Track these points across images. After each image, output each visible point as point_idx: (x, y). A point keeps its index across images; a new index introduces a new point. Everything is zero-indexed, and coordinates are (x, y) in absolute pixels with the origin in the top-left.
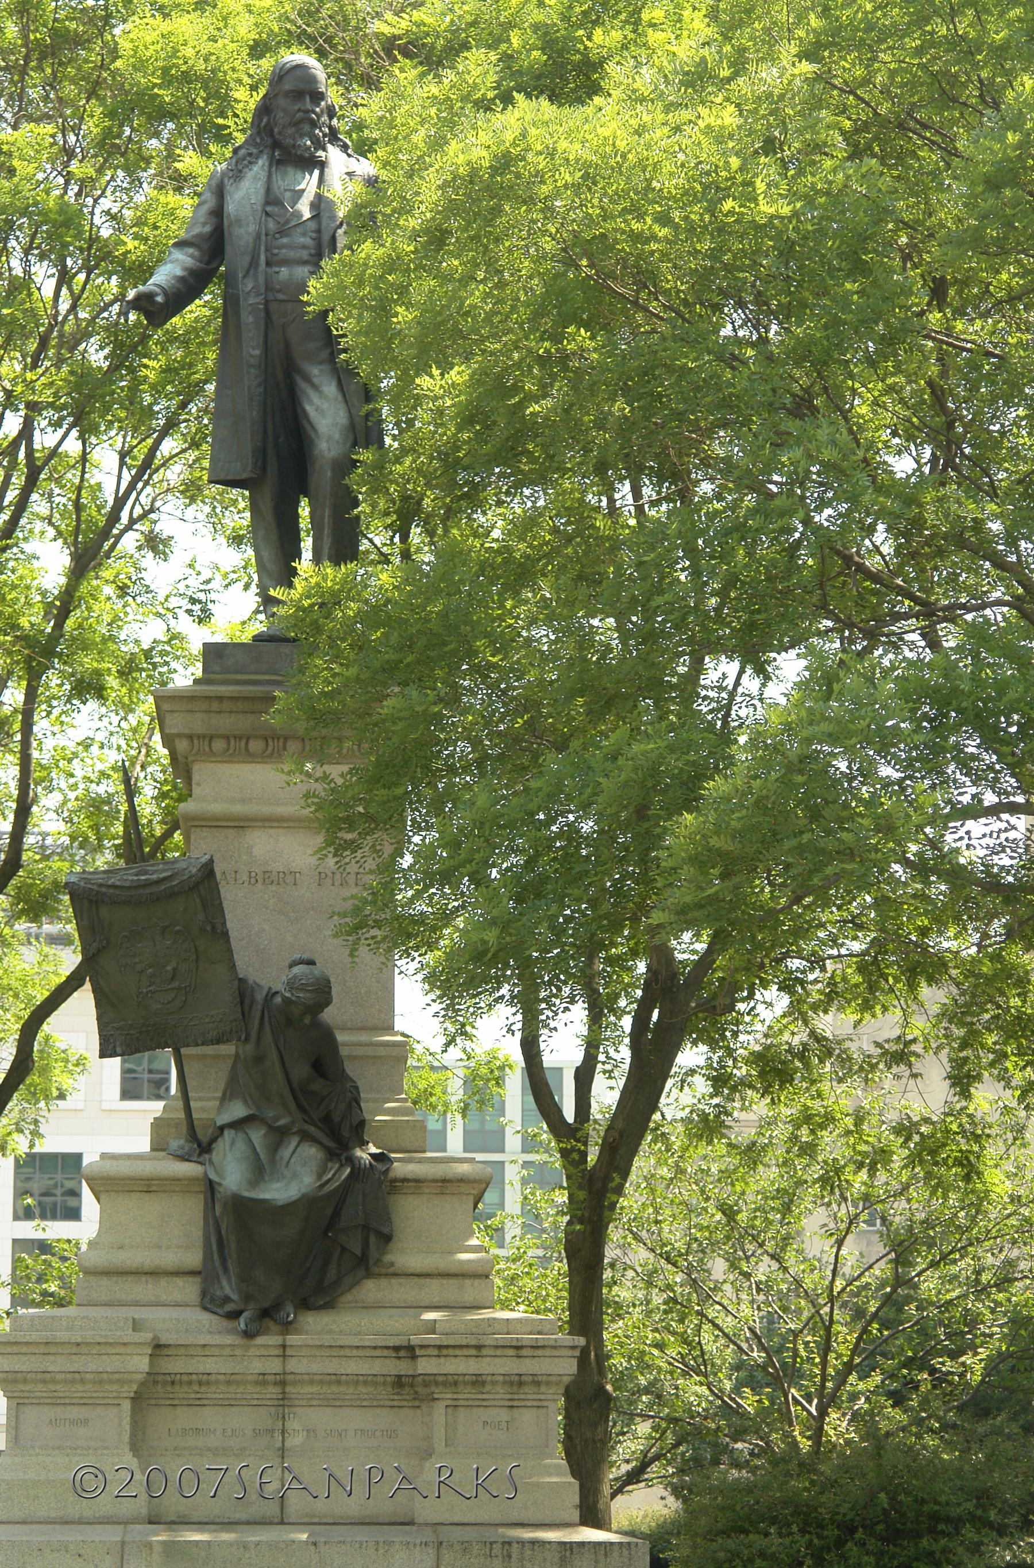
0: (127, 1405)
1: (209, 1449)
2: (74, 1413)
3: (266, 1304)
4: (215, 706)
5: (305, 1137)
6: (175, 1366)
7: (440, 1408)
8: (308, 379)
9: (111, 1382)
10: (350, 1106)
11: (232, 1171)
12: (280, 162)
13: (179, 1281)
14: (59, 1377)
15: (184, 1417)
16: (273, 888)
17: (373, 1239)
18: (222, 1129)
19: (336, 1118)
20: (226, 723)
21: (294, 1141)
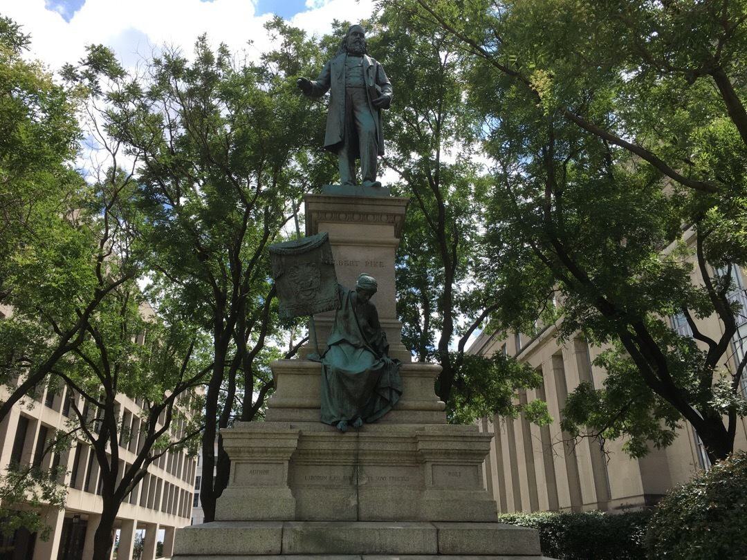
0: (286, 464)
1: (324, 486)
2: (262, 467)
3: (350, 419)
4: (327, 200)
5: (366, 349)
6: (311, 446)
7: (429, 465)
8: (357, 111)
9: (280, 452)
10: (382, 340)
11: (335, 359)
12: (349, 56)
13: (310, 411)
14: (256, 449)
15: (313, 471)
16: (348, 267)
17: (394, 393)
18: (330, 347)
19: (377, 344)
20: (331, 207)
21: (362, 350)
